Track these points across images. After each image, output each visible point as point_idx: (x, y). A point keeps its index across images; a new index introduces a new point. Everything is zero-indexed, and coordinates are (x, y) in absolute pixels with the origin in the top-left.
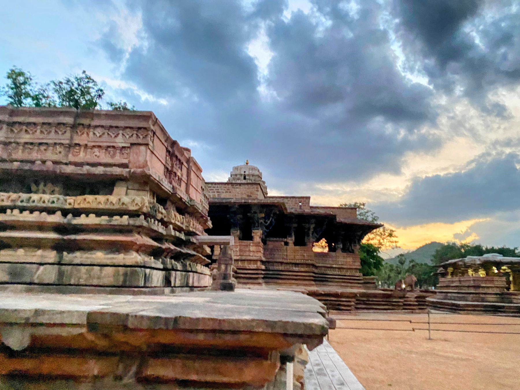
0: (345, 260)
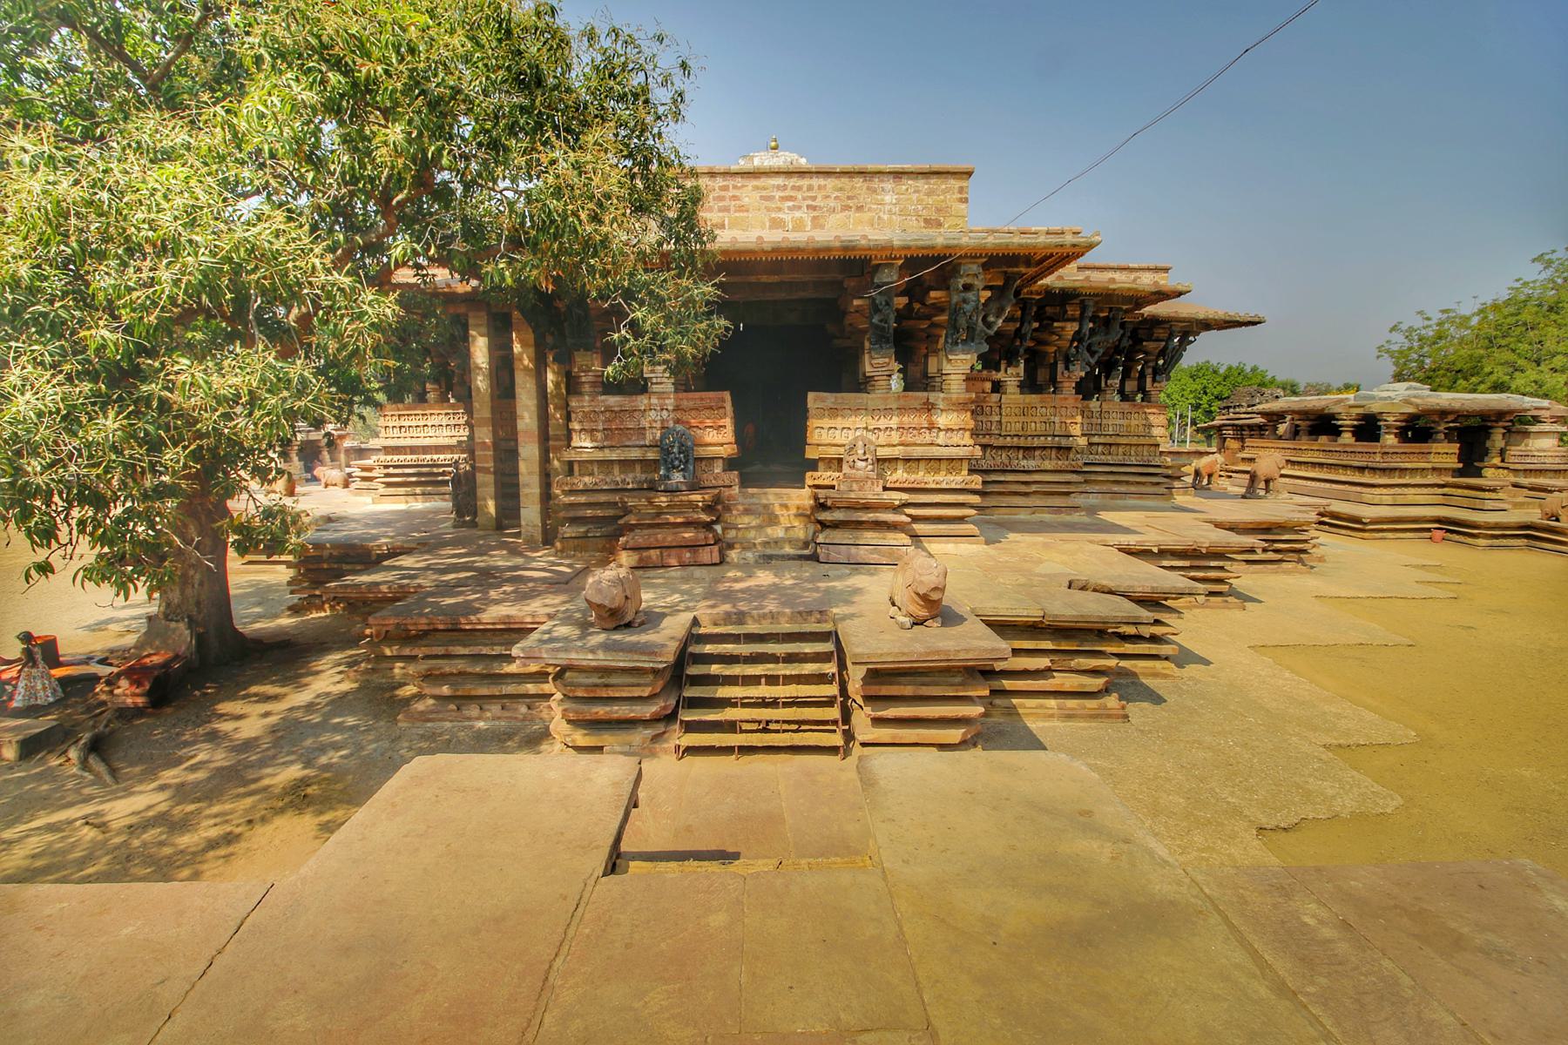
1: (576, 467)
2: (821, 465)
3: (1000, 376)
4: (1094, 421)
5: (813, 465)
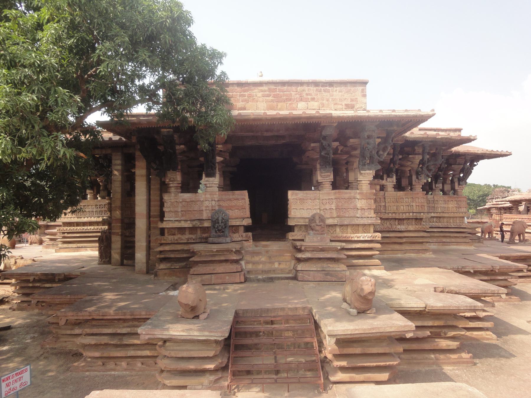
0: (445, 205)
1: (166, 231)
2: (296, 229)
3: (384, 182)
4: (431, 205)
5: (291, 229)
